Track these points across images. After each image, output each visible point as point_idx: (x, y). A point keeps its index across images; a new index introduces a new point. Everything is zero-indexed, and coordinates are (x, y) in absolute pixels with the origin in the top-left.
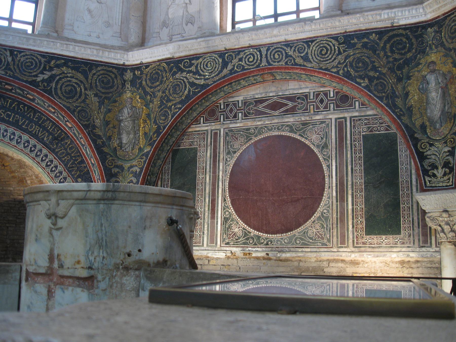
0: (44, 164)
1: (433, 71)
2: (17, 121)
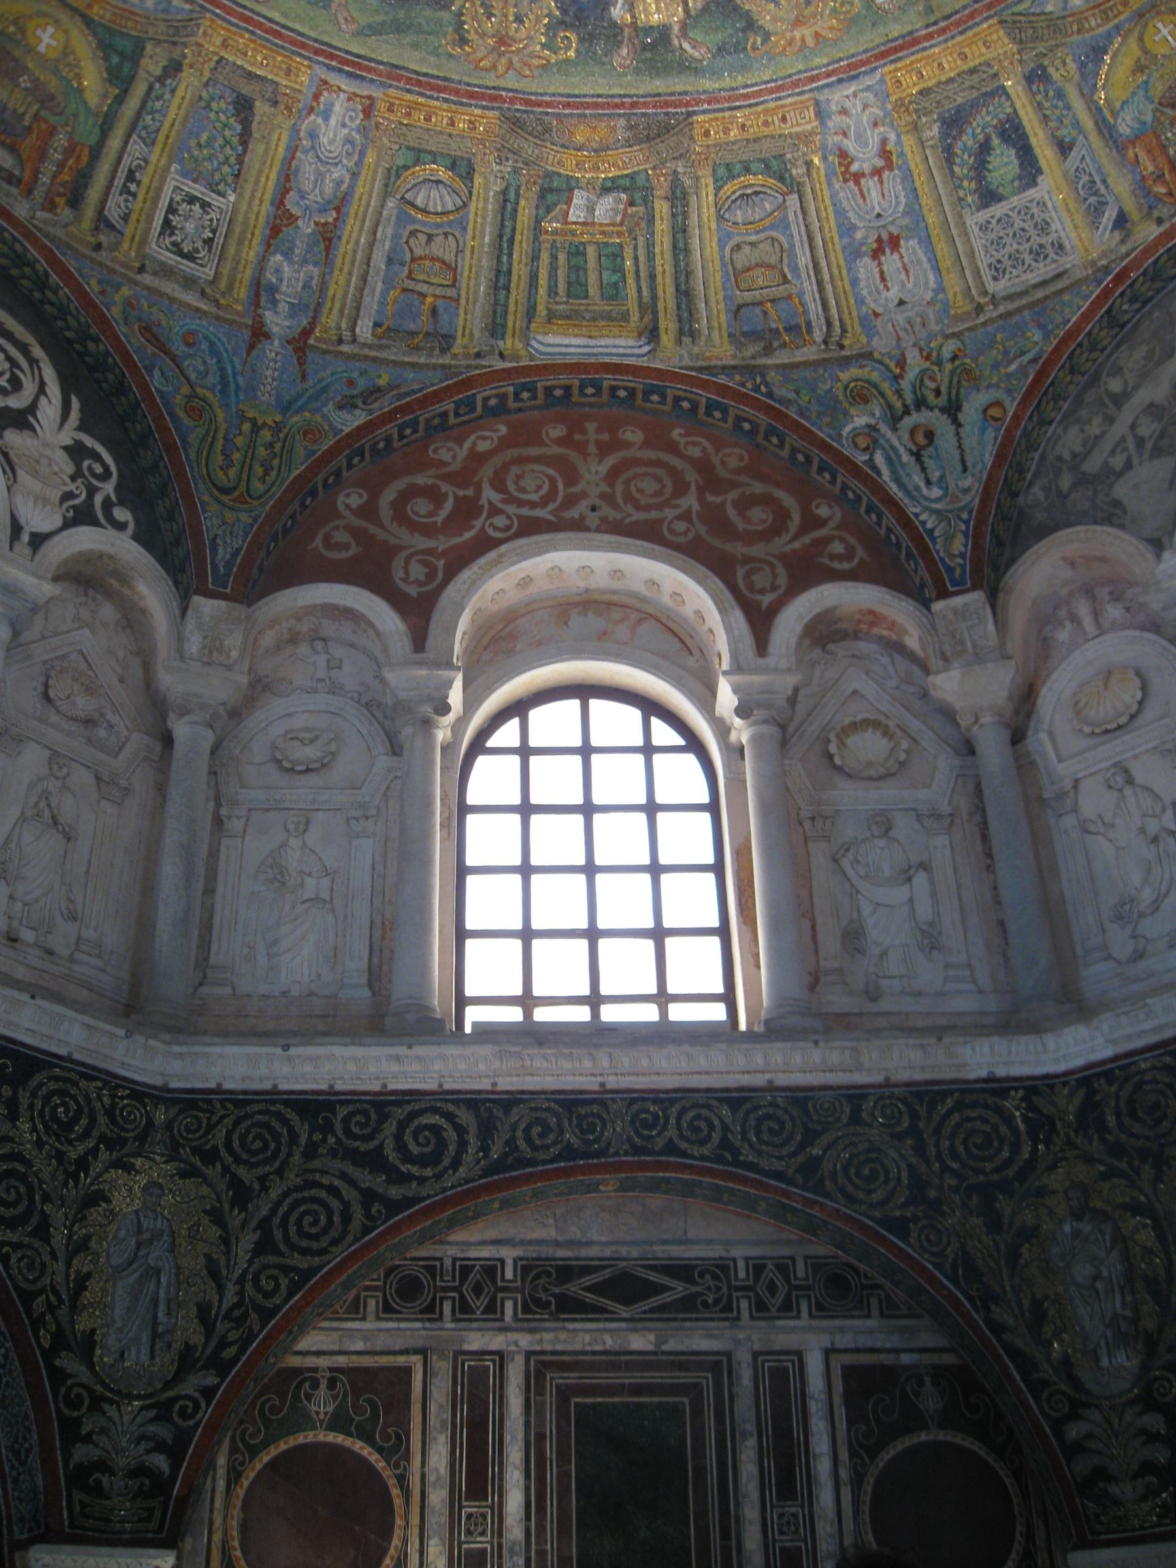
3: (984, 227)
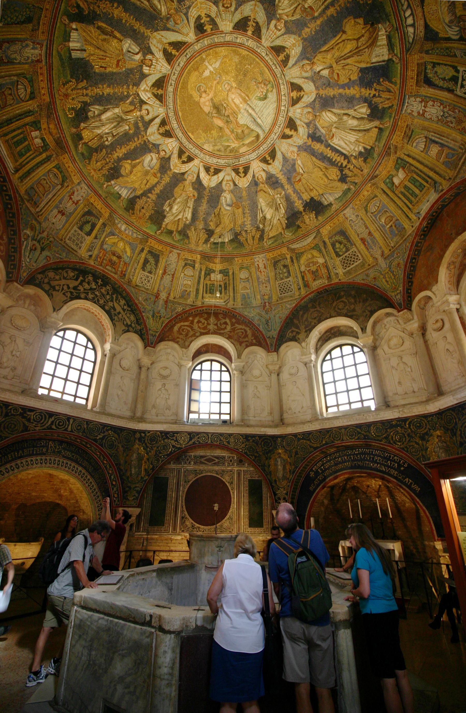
0: (87, 485)
1: (280, 457)
2: (77, 459)
3: (75, 231)
